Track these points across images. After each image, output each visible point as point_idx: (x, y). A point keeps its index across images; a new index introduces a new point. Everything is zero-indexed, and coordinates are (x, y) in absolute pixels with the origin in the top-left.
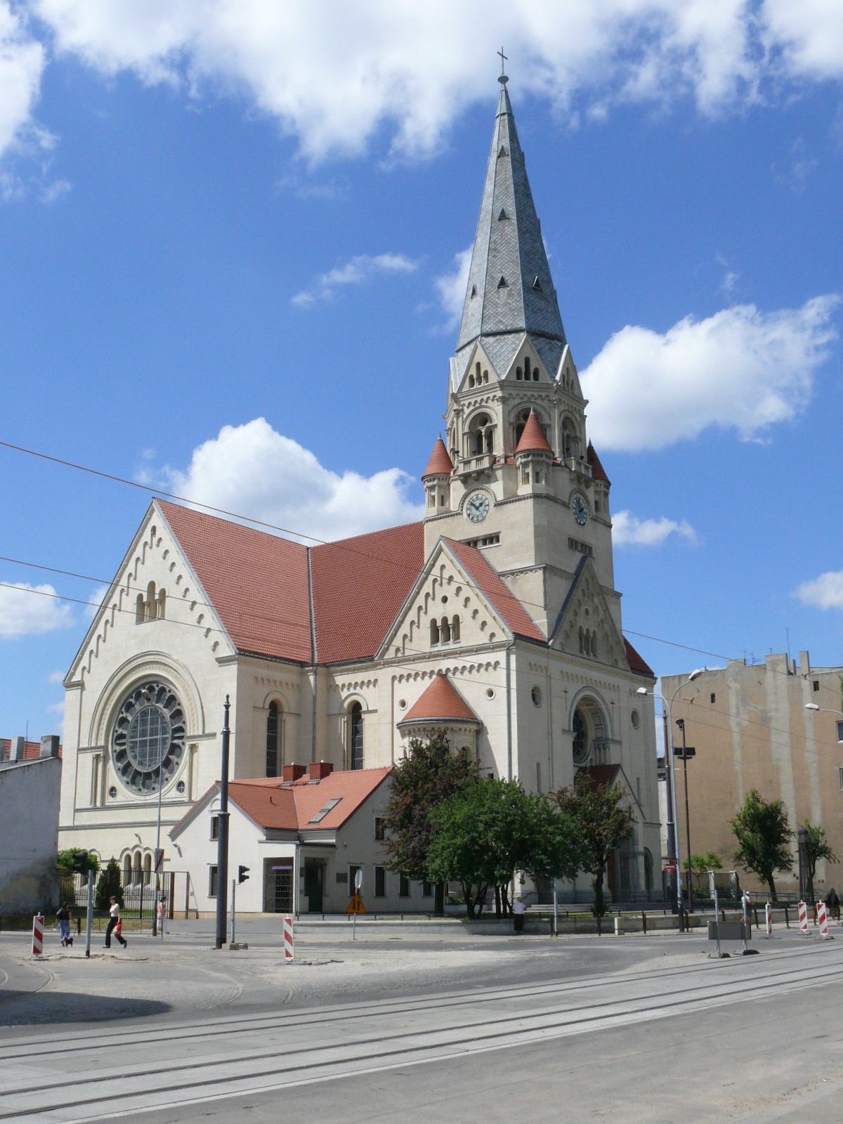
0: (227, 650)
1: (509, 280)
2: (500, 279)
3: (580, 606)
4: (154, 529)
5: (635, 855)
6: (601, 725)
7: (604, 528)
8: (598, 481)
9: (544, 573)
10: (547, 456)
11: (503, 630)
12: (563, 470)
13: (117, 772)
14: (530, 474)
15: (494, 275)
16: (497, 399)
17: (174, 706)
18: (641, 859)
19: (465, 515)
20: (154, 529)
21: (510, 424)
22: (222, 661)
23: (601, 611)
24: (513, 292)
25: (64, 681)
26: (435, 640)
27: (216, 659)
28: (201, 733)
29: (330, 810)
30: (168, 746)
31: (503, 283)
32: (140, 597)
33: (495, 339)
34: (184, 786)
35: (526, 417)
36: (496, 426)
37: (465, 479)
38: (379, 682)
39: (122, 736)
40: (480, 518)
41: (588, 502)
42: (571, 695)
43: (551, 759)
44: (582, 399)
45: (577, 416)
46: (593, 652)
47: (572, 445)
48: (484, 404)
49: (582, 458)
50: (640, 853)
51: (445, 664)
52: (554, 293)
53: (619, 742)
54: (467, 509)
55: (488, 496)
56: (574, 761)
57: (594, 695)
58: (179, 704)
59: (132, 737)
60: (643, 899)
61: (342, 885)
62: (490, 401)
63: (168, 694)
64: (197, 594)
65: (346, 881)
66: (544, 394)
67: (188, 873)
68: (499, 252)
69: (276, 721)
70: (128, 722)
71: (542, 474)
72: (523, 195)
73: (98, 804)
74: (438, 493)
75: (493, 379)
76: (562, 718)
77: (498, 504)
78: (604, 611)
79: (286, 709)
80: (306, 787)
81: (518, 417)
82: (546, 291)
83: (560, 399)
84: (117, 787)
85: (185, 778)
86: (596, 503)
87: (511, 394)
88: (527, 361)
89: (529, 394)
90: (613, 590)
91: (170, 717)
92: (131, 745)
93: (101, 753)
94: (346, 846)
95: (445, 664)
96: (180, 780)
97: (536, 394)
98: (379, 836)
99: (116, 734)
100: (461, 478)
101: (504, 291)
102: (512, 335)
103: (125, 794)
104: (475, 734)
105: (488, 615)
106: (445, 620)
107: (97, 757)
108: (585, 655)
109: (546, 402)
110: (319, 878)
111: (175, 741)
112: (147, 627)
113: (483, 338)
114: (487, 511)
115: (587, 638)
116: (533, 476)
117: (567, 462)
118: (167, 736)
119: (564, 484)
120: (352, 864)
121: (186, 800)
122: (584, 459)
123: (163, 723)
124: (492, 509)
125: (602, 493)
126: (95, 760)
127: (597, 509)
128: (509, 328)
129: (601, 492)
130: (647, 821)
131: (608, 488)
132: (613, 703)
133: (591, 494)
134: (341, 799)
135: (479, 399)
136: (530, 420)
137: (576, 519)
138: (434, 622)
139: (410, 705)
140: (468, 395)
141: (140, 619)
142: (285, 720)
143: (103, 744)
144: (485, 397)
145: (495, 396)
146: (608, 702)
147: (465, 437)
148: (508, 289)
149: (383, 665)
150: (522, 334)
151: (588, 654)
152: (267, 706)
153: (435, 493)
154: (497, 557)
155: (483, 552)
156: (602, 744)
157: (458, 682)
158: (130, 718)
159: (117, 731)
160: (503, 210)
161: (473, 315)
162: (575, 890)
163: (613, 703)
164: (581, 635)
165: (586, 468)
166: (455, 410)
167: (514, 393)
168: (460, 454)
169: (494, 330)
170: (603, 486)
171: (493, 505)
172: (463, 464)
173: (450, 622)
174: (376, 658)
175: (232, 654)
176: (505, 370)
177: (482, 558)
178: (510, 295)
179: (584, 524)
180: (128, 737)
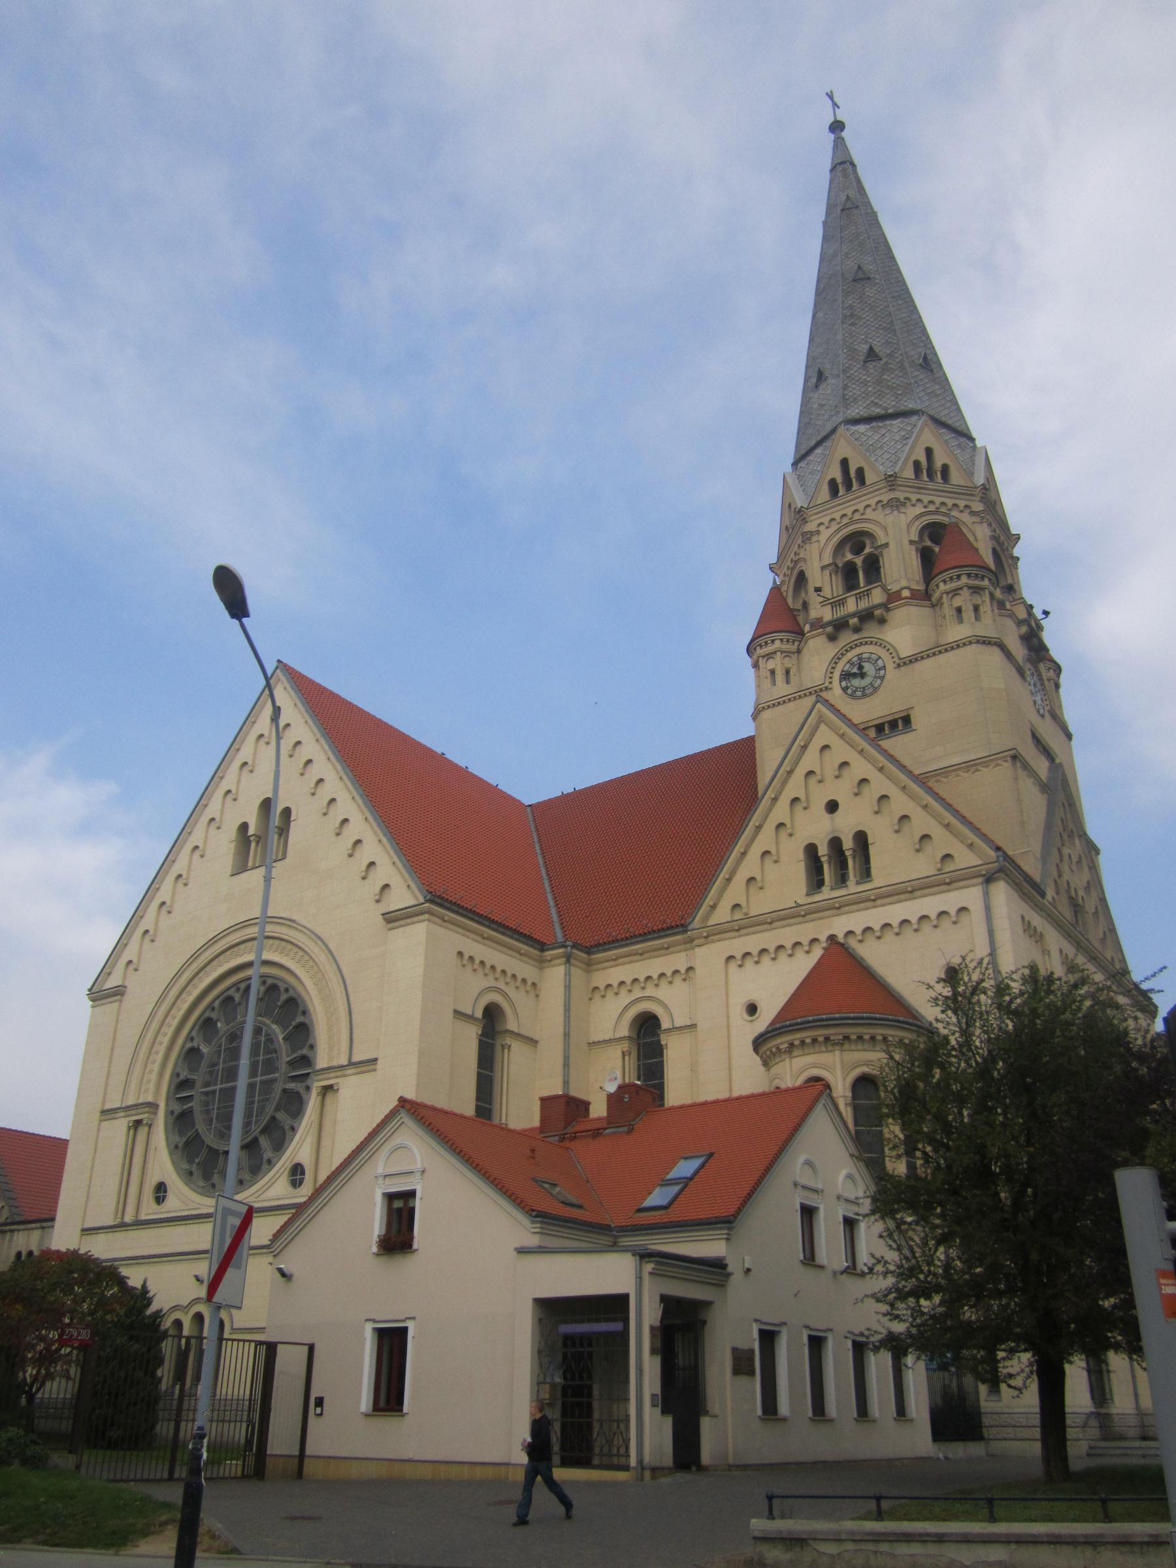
0: (404, 895)
13: (171, 1154)
22: (393, 919)
25: (90, 990)
26: (816, 881)
28: (344, 1061)
29: (691, 1179)
31: (872, 355)
32: (244, 827)
33: (868, 427)
34: (303, 1173)
36: (886, 545)
38: (699, 971)
48: (857, 516)
51: (839, 925)
59: (207, 1084)
61: (744, 1379)
62: (869, 510)
63: (284, 997)
64: (350, 805)
65: (751, 1373)
66: (962, 504)
67: (311, 1348)
69: (491, 1047)
75: (870, 478)
78: (1090, 868)
79: (512, 1025)
88: (929, 452)
89: (938, 500)
91: (284, 1039)
92: (203, 1098)
94: (748, 1270)
96: (297, 1160)
97: (950, 502)
105: (933, 822)
106: (835, 843)
107: (138, 1123)
111: (291, 1085)
114: (882, 678)
118: (277, 1075)
120: (762, 1323)
124: (891, 673)
126: (132, 1131)
128: (890, 411)
134: (711, 1155)
135: (849, 512)
138: (811, 850)
141: (241, 866)
142: (510, 1046)
147: (827, 572)
148: (882, 362)
149: (706, 937)
150: (915, 418)
152: (479, 1014)
157: (873, 954)
159: (178, 1075)
167: (914, 497)
169: (865, 415)
173: (848, 844)
175: (412, 902)
180: (198, 1084)
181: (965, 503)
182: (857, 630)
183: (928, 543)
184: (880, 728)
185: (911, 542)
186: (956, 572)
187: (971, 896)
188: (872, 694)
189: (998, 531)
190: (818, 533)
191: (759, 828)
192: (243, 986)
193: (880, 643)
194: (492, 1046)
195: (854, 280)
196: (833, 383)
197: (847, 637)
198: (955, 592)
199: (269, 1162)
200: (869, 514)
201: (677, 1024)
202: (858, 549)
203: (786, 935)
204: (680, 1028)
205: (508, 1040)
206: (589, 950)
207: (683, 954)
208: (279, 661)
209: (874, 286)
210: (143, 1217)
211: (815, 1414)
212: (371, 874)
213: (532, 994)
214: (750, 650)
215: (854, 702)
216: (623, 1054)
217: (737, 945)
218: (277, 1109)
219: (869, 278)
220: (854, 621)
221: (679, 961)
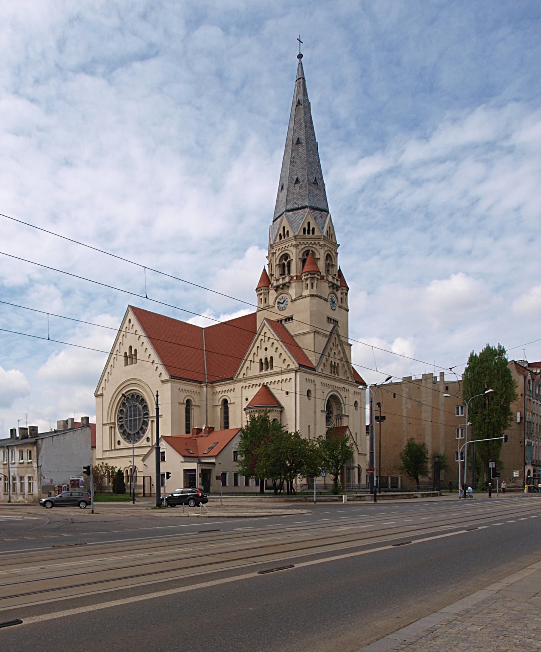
1: (301, 179)
2: (296, 179)
3: (331, 351)
4: (130, 320)
5: (353, 468)
6: (340, 408)
7: (345, 311)
8: (343, 288)
9: (314, 334)
10: (317, 274)
11: (294, 363)
12: (325, 282)
13: (120, 434)
14: (309, 285)
15: (293, 177)
16: (293, 246)
17: (143, 404)
18: (356, 470)
19: (276, 307)
20: (130, 320)
21: (299, 259)
23: (342, 353)
24: (302, 186)
27: (161, 381)
30: (142, 421)
31: (297, 181)
33: (292, 213)
34: (149, 439)
35: (307, 255)
37: (277, 288)
38: (236, 390)
39: (121, 418)
40: (284, 309)
41: (337, 298)
42: (326, 394)
43: (315, 424)
44: (337, 244)
45: (333, 253)
46: (337, 373)
47: (330, 269)
48: (286, 249)
49: (335, 275)
50: (356, 467)
52: (324, 185)
53: (348, 416)
54: (278, 304)
55: (288, 297)
56: (326, 425)
57: (337, 394)
58: (146, 402)
59: (126, 418)
60: (356, 488)
62: (289, 247)
63: (141, 398)
64: (151, 350)
66: (317, 242)
68: (296, 163)
70: (124, 411)
71: (315, 285)
72: (309, 128)
73: (113, 448)
74: (264, 297)
75: (291, 235)
76: (322, 405)
77: (293, 301)
79: (193, 404)
80: (202, 438)
81: (303, 255)
82: (320, 184)
83: (325, 244)
84: (120, 440)
85: (150, 436)
86: (341, 299)
87: (300, 243)
89: (309, 242)
90: (348, 343)
91: (142, 408)
93: (113, 426)
95: (266, 380)
97: (313, 242)
98: (235, 460)
99: (119, 417)
100: (275, 288)
101: (298, 185)
102: (301, 210)
103: (124, 444)
104: (280, 413)
107: (111, 427)
108: (333, 375)
109: (318, 246)
110: (208, 478)
111: (145, 419)
112: (129, 367)
113: (287, 213)
114: (287, 305)
115: (334, 366)
116: (310, 285)
117: (327, 278)
118: (141, 417)
119: (325, 289)
121: (150, 445)
122: (336, 276)
123: (139, 411)
125: (345, 294)
127: (342, 302)
128: (300, 206)
129: (344, 293)
130: (359, 453)
131: (348, 291)
132: (345, 398)
133: (339, 294)
135: (284, 247)
136: (309, 256)
137: (331, 307)
139: (249, 400)
140: (278, 244)
143: (113, 421)
144: (287, 245)
145: (292, 244)
146: (343, 397)
148: (300, 184)
150: (306, 209)
151: (335, 374)
152: (185, 402)
153: (262, 297)
154: (291, 327)
155: (285, 325)
156: (340, 417)
158: (124, 410)
159: (119, 416)
160: (298, 138)
161: (282, 200)
162: (325, 483)
163: (345, 398)
164: (331, 365)
165: (337, 280)
166: (272, 253)
168: (274, 276)
169: (292, 208)
170: (345, 290)
171: (290, 301)
172: (275, 281)
174: (234, 379)
175: (167, 378)
176: (297, 230)
177: (284, 328)
178: (301, 187)
179: (335, 310)
180: (124, 418)
181: (318, 241)
182: (282, 289)
183: (306, 257)
184: (286, 320)
185: (299, 259)
186: (307, 273)
187: (292, 375)
188: (284, 309)
189: (330, 246)
190: (276, 253)
191: (250, 354)
192: (131, 395)
193: (287, 294)
194: (189, 409)
195: (296, 144)
196: (285, 191)
197: (280, 291)
198: (306, 279)
199: (142, 436)
200: (289, 248)
201: (232, 402)
202: (286, 260)
203: (254, 382)
204: (232, 403)
205: (193, 407)
206: (212, 383)
207: (233, 385)
208: (129, 305)
209: (302, 147)
210: (116, 448)
211: (245, 485)
212: (157, 369)
213: (199, 395)
214: (256, 290)
215: (280, 311)
216: (220, 409)
217: (244, 384)
218: (143, 424)
219: (301, 143)
220: (281, 286)
221: (231, 387)
